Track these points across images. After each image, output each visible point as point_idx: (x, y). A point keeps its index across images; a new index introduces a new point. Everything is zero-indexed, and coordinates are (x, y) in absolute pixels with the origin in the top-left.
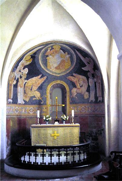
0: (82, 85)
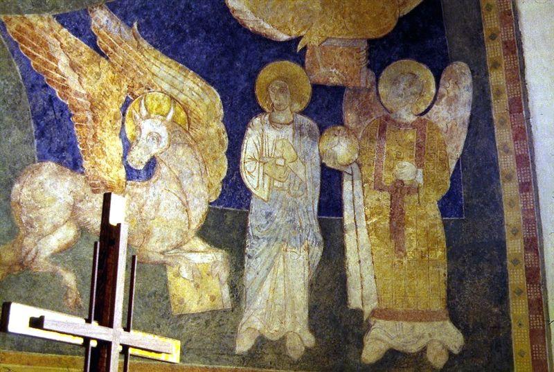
0: (152, 165)
